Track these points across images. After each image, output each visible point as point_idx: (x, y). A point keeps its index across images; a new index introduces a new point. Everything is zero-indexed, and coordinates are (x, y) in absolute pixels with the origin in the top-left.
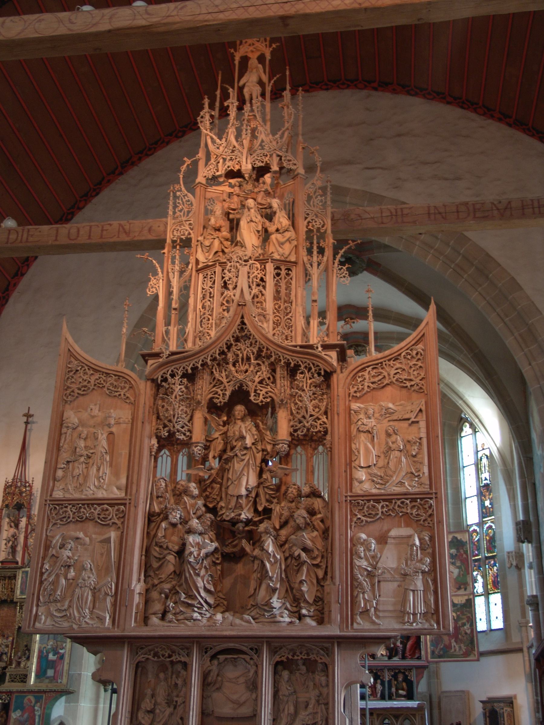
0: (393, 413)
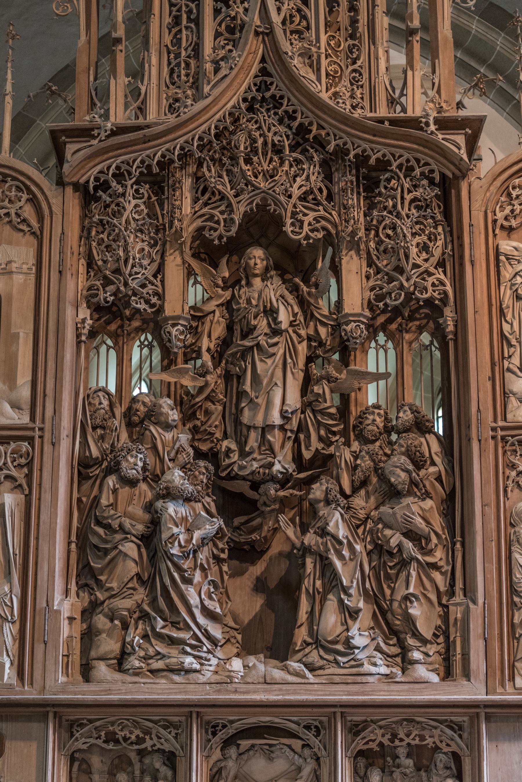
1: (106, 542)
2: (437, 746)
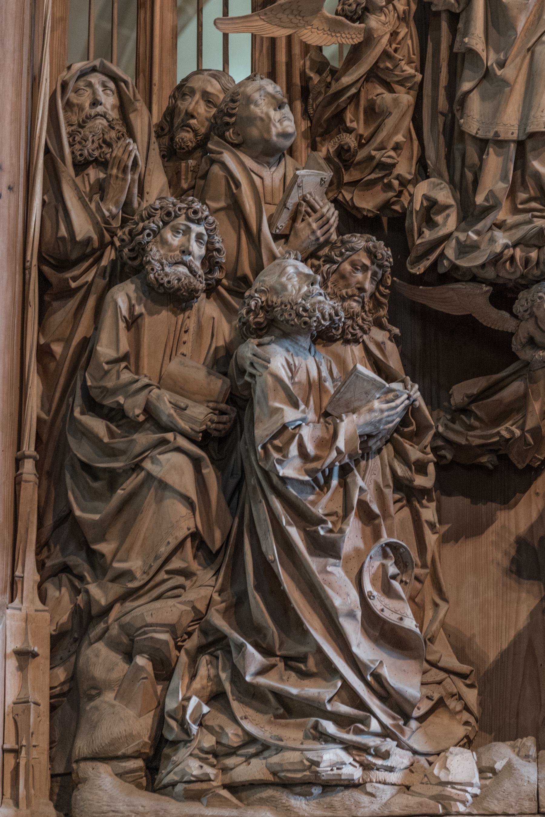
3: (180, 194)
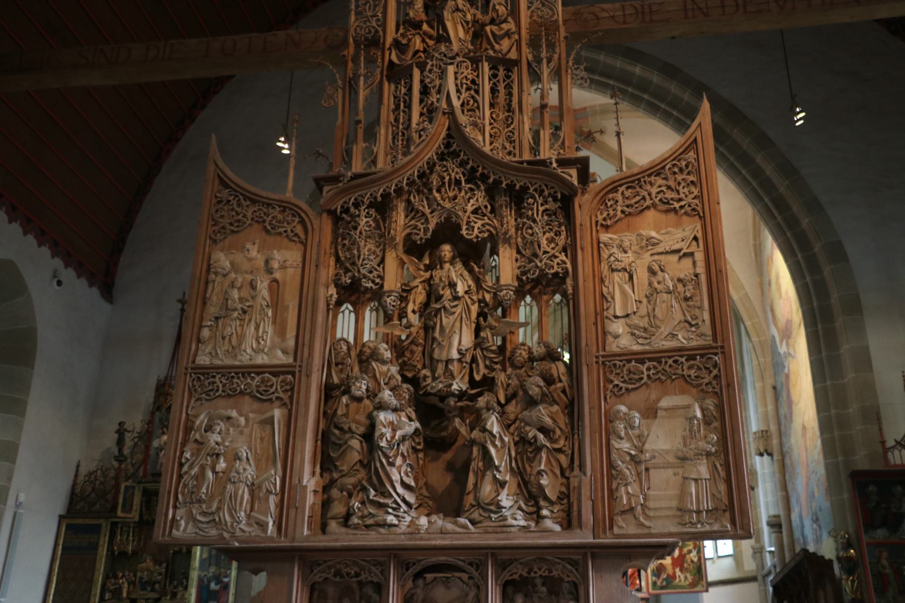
0: (657, 244)
1: (340, 439)
2: (560, 577)
3: (361, 371)
